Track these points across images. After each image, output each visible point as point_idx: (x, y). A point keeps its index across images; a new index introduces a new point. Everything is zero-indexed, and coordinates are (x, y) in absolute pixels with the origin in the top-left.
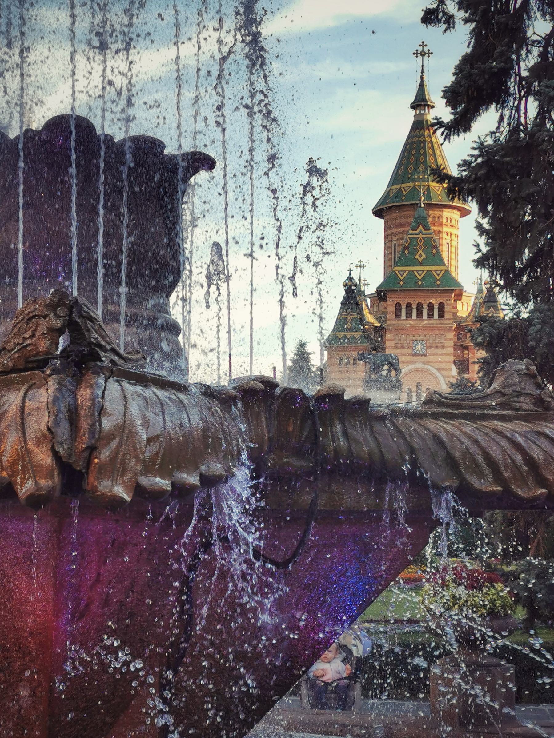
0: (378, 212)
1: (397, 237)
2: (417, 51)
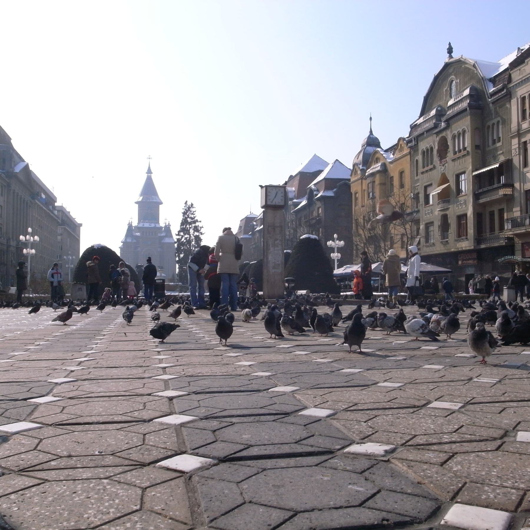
0: (136, 203)
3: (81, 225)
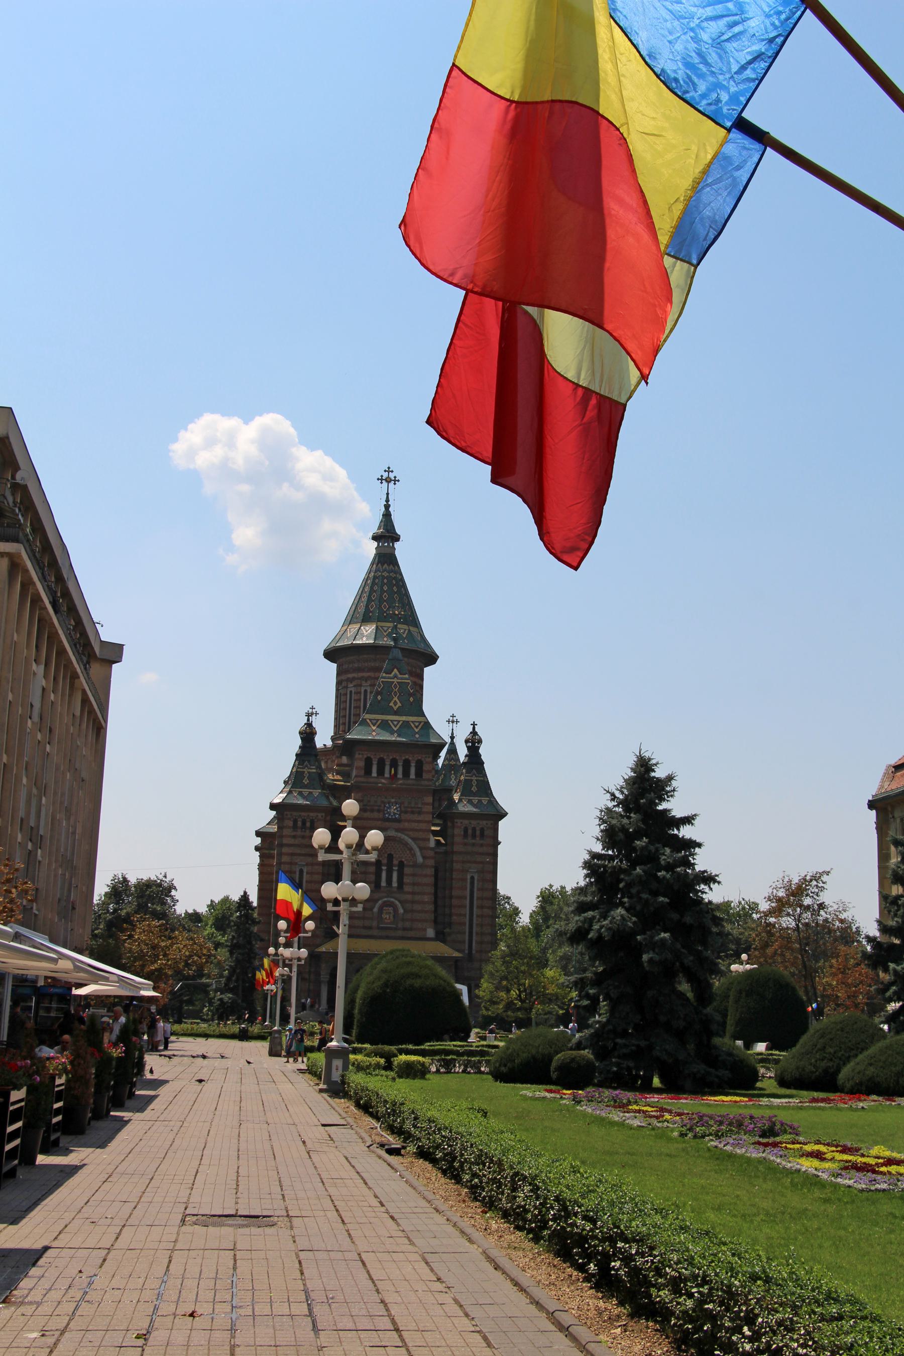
0: (331, 654)
1: (354, 683)
2: (382, 476)
3: (115, 653)
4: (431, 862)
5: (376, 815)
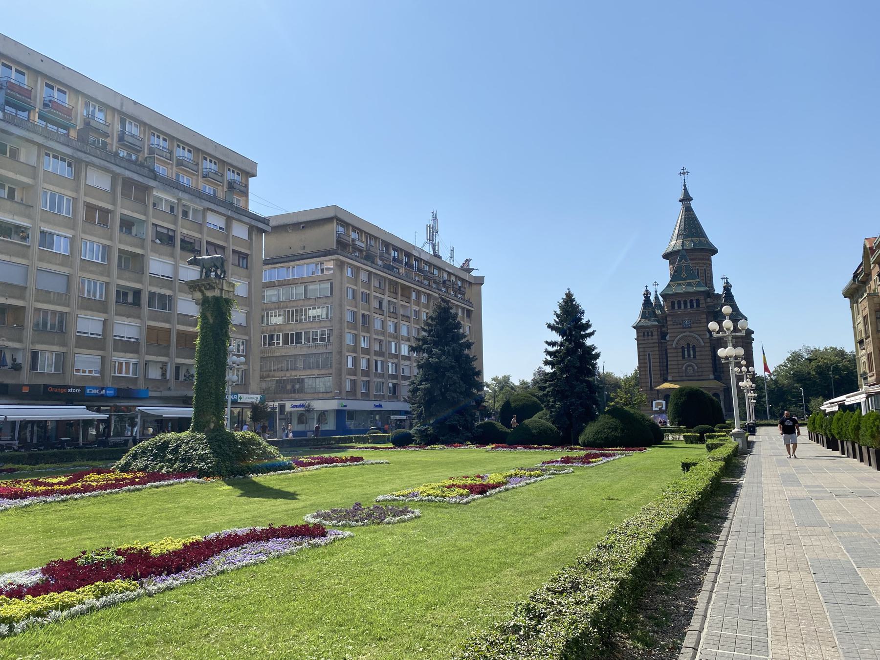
0: (666, 256)
3: (480, 281)
4: (708, 345)
5: (679, 326)
